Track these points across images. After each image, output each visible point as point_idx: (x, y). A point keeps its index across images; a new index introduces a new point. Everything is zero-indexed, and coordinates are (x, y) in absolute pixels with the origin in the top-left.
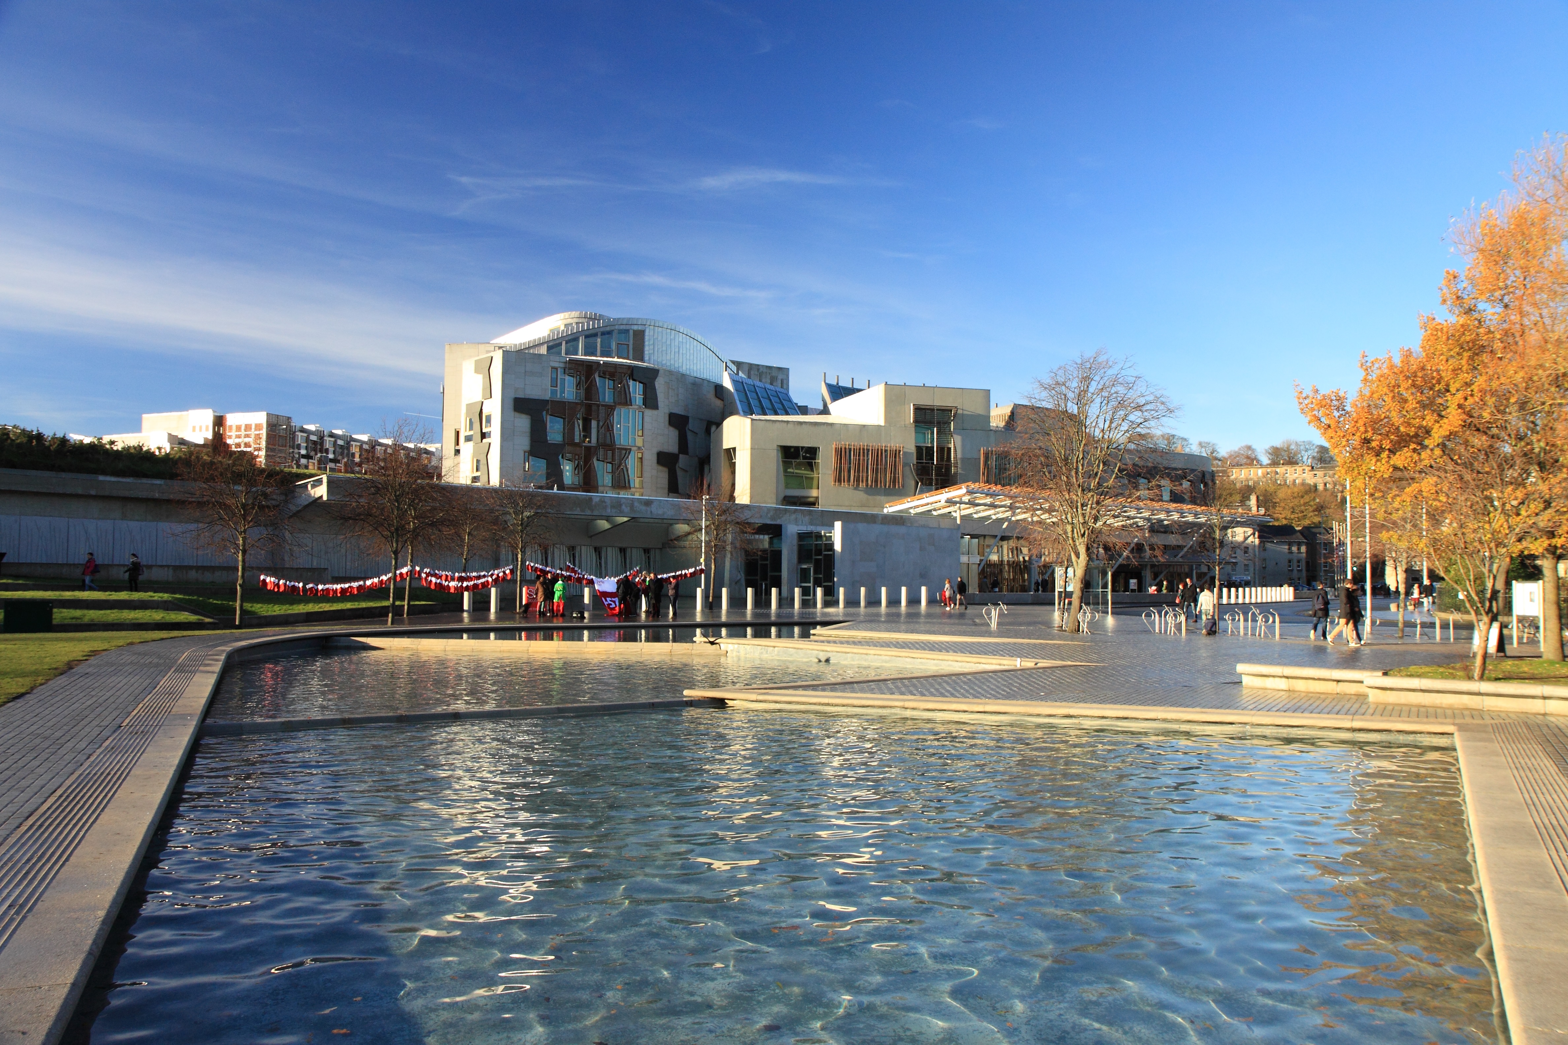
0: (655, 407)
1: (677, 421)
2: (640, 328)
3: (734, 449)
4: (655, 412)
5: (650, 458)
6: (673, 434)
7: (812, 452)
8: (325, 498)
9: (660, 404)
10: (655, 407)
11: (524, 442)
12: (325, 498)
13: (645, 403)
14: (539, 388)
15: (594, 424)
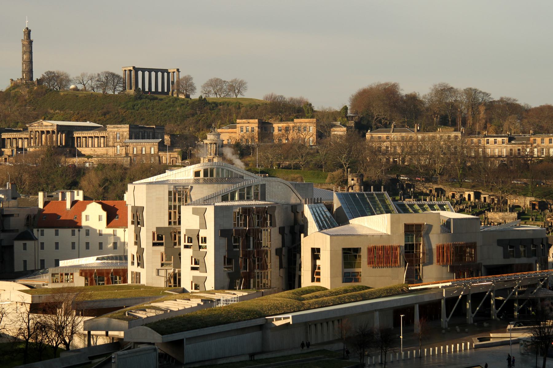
0: (275, 226)
1: (282, 231)
2: (264, 183)
3: (318, 250)
4: (275, 228)
5: (273, 252)
6: (280, 236)
7: (357, 250)
8: (291, 323)
9: (277, 224)
10: (275, 226)
11: (224, 252)
12: (291, 323)
13: (271, 225)
14: (230, 225)
15: (251, 239)
